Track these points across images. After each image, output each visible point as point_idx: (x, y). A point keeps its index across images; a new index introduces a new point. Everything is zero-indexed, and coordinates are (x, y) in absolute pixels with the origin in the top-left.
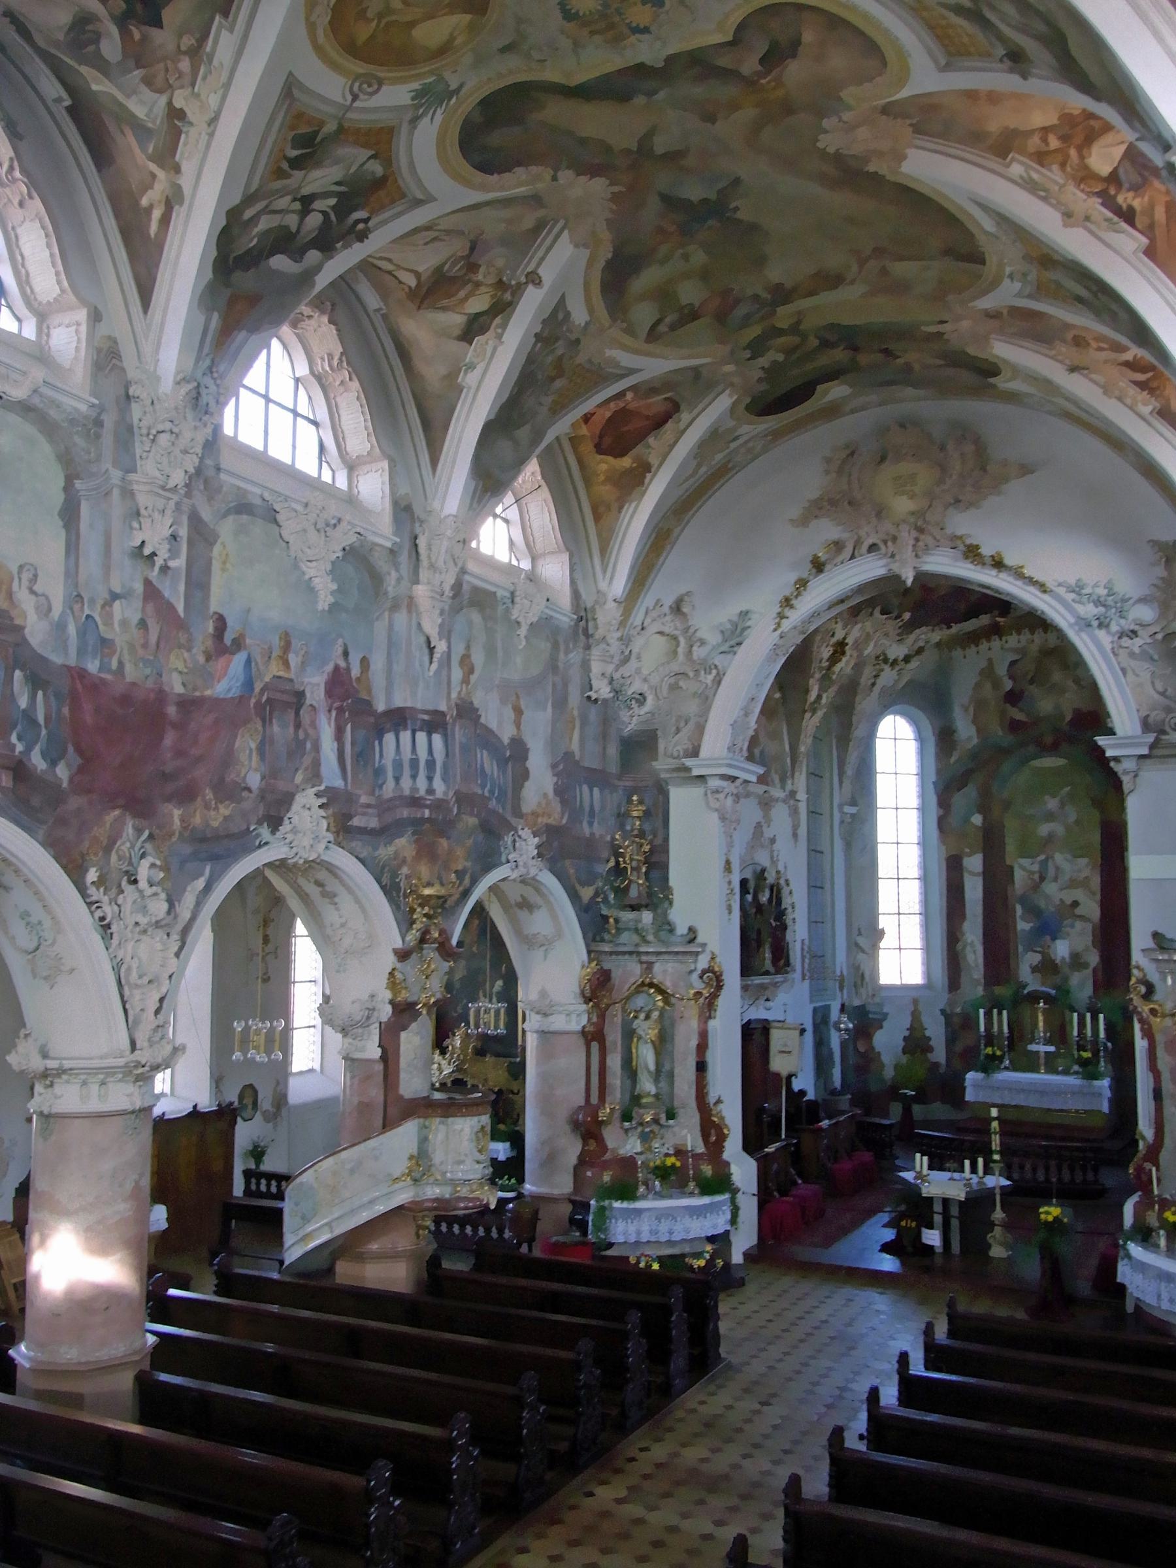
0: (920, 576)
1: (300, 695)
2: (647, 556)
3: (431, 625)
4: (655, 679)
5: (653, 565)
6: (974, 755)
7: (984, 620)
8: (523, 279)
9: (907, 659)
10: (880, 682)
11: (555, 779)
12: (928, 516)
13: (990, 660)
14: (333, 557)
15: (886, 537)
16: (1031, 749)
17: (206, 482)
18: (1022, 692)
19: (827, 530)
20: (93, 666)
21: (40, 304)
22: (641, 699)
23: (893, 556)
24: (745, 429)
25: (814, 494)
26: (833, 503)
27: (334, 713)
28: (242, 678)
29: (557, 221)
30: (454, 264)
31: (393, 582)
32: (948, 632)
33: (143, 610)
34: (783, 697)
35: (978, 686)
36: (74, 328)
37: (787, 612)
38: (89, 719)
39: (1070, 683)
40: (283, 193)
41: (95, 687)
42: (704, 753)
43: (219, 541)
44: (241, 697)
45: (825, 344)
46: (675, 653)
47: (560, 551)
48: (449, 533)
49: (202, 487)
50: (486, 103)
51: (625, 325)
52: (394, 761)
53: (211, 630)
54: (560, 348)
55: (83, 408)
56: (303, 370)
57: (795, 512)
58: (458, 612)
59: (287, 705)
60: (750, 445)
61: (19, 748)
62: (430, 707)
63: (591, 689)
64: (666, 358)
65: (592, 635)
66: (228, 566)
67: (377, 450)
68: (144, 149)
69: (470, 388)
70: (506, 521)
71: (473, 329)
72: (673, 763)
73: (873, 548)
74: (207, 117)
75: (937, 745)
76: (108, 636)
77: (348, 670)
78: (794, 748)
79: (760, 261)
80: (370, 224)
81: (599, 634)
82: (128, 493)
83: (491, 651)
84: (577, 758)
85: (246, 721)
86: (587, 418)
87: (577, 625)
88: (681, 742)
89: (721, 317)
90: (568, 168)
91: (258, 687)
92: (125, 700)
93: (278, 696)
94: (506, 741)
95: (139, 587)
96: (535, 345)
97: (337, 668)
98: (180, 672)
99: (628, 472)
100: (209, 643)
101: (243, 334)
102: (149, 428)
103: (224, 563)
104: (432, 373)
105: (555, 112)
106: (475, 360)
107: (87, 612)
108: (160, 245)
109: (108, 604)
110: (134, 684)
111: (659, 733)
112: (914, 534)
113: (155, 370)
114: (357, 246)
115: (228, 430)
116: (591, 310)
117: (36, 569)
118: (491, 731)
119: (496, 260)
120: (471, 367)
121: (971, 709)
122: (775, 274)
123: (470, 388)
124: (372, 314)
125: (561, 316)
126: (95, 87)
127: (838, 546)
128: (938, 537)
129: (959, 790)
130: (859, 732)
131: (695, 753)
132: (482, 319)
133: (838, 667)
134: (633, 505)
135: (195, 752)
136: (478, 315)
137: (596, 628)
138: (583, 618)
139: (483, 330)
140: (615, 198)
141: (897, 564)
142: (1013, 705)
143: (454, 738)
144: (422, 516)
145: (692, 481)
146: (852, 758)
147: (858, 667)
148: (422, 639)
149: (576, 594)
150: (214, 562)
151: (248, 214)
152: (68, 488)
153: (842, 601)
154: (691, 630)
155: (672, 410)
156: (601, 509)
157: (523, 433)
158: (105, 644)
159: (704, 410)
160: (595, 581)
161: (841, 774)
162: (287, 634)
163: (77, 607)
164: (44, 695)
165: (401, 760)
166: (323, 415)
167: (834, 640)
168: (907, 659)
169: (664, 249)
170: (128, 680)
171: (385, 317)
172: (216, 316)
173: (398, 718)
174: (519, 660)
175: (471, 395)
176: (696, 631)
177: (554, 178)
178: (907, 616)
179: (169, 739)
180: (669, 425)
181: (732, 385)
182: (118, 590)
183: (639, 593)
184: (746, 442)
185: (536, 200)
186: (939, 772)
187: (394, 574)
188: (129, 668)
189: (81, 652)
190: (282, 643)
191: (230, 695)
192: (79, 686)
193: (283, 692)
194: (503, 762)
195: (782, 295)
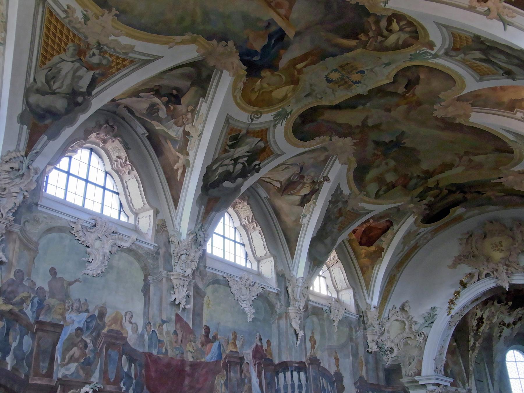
0: (511, 286)
1: (242, 358)
2: (386, 287)
3: (296, 324)
4: (397, 341)
5: (390, 291)
8: (322, 180)
10: (503, 335)
11: (356, 390)
12: (510, 259)
14: (253, 298)
15: (493, 270)
17: (200, 272)
19: (465, 269)
20: (155, 352)
21: (136, 210)
22: (391, 350)
23: (497, 278)
24: (422, 230)
25: (457, 254)
26: (466, 257)
27: (257, 365)
28: (217, 353)
30: (294, 177)
31: (279, 307)
33: (175, 327)
34: (458, 344)
36: (149, 217)
37: (453, 306)
38: (153, 374)
40: (226, 158)
41: (156, 361)
42: (423, 374)
43: (206, 296)
44: (217, 361)
45: (451, 192)
46: (404, 328)
47: (348, 288)
48: (300, 285)
49: (199, 275)
51: (365, 193)
52: (284, 386)
53: (203, 333)
54: (340, 205)
55: (152, 248)
56: (238, 224)
57: (450, 262)
58: (307, 318)
59: (236, 363)
60: (425, 236)
61: (124, 388)
62: (298, 360)
63: (368, 348)
64: (384, 204)
65: (367, 323)
66: (210, 305)
67: (268, 253)
68: (174, 148)
69: (305, 224)
70: (325, 278)
71: (304, 201)
72: (410, 379)
73: (487, 275)
74: (198, 134)
76: (161, 339)
77: (262, 346)
78: (467, 369)
79: (418, 162)
80: (261, 165)
81: (369, 322)
82: (169, 280)
83: (322, 334)
84: (366, 379)
85: (219, 372)
86: (354, 232)
87: (359, 319)
88: (412, 369)
89: (405, 186)
91: (224, 356)
92: (168, 365)
93: (232, 359)
94: (333, 374)
95: (174, 317)
96: (330, 204)
97: (257, 346)
98: (191, 352)
99: (375, 252)
100: (203, 339)
101: (214, 212)
102: (177, 253)
103: (209, 305)
104: (289, 220)
106: (306, 214)
107: (152, 329)
108: (181, 183)
109: (161, 325)
110: (172, 358)
111: (402, 365)
112: (505, 267)
113: (179, 231)
114: (256, 174)
115: (209, 251)
117: (132, 313)
118: (325, 369)
119: (311, 173)
120: (305, 216)
122: (425, 166)
123: (305, 224)
124: (264, 199)
125: (339, 192)
126: (157, 128)
127: (471, 275)
128: (517, 268)
130: (497, 359)
131: (419, 373)
132: (308, 196)
133: (481, 329)
134: (378, 265)
135: (198, 386)
136: (305, 196)
137: (368, 320)
138: (362, 316)
139: (308, 201)
140: (355, 144)
141: (500, 281)
143: (310, 373)
144: (289, 279)
145: (402, 253)
146: (496, 372)
147: (491, 328)
148: (293, 331)
149: (357, 306)
150: (204, 305)
151: (214, 167)
152: (145, 279)
153: (477, 300)
154: (410, 318)
155: (390, 224)
156: (365, 269)
157: (328, 241)
158: (160, 341)
159: (404, 223)
160: (365, 300)
161: (492, 380)
162: (235, 333)
163: (148, 327)
164: (135, 365)
165: (287, 385)
166: (246, 242)
167: (477, 317)
168: (514, 323)
169: (377, 162)
170: (169, 356)
171: (269, 200)
172: (203, 207)
173: (285, 366)
174: (335, 337)
175: (305, 227)
176: (412, 318)
177: (331, 140)
178: (510, 303)
179: (187, 382)
180: (389, 231)
181: (414, 212)
182: (165, 319)
183: (385, 303)
184: (423, 235)
185: (324, 149)
187: (279, 304)
188: (170, 352)
189: (150, 346)
190: (233, 337)
191: (212, 360)
192: (149, 361)
193: (235, 357)
194: (332, 383)
195: (429, 174)
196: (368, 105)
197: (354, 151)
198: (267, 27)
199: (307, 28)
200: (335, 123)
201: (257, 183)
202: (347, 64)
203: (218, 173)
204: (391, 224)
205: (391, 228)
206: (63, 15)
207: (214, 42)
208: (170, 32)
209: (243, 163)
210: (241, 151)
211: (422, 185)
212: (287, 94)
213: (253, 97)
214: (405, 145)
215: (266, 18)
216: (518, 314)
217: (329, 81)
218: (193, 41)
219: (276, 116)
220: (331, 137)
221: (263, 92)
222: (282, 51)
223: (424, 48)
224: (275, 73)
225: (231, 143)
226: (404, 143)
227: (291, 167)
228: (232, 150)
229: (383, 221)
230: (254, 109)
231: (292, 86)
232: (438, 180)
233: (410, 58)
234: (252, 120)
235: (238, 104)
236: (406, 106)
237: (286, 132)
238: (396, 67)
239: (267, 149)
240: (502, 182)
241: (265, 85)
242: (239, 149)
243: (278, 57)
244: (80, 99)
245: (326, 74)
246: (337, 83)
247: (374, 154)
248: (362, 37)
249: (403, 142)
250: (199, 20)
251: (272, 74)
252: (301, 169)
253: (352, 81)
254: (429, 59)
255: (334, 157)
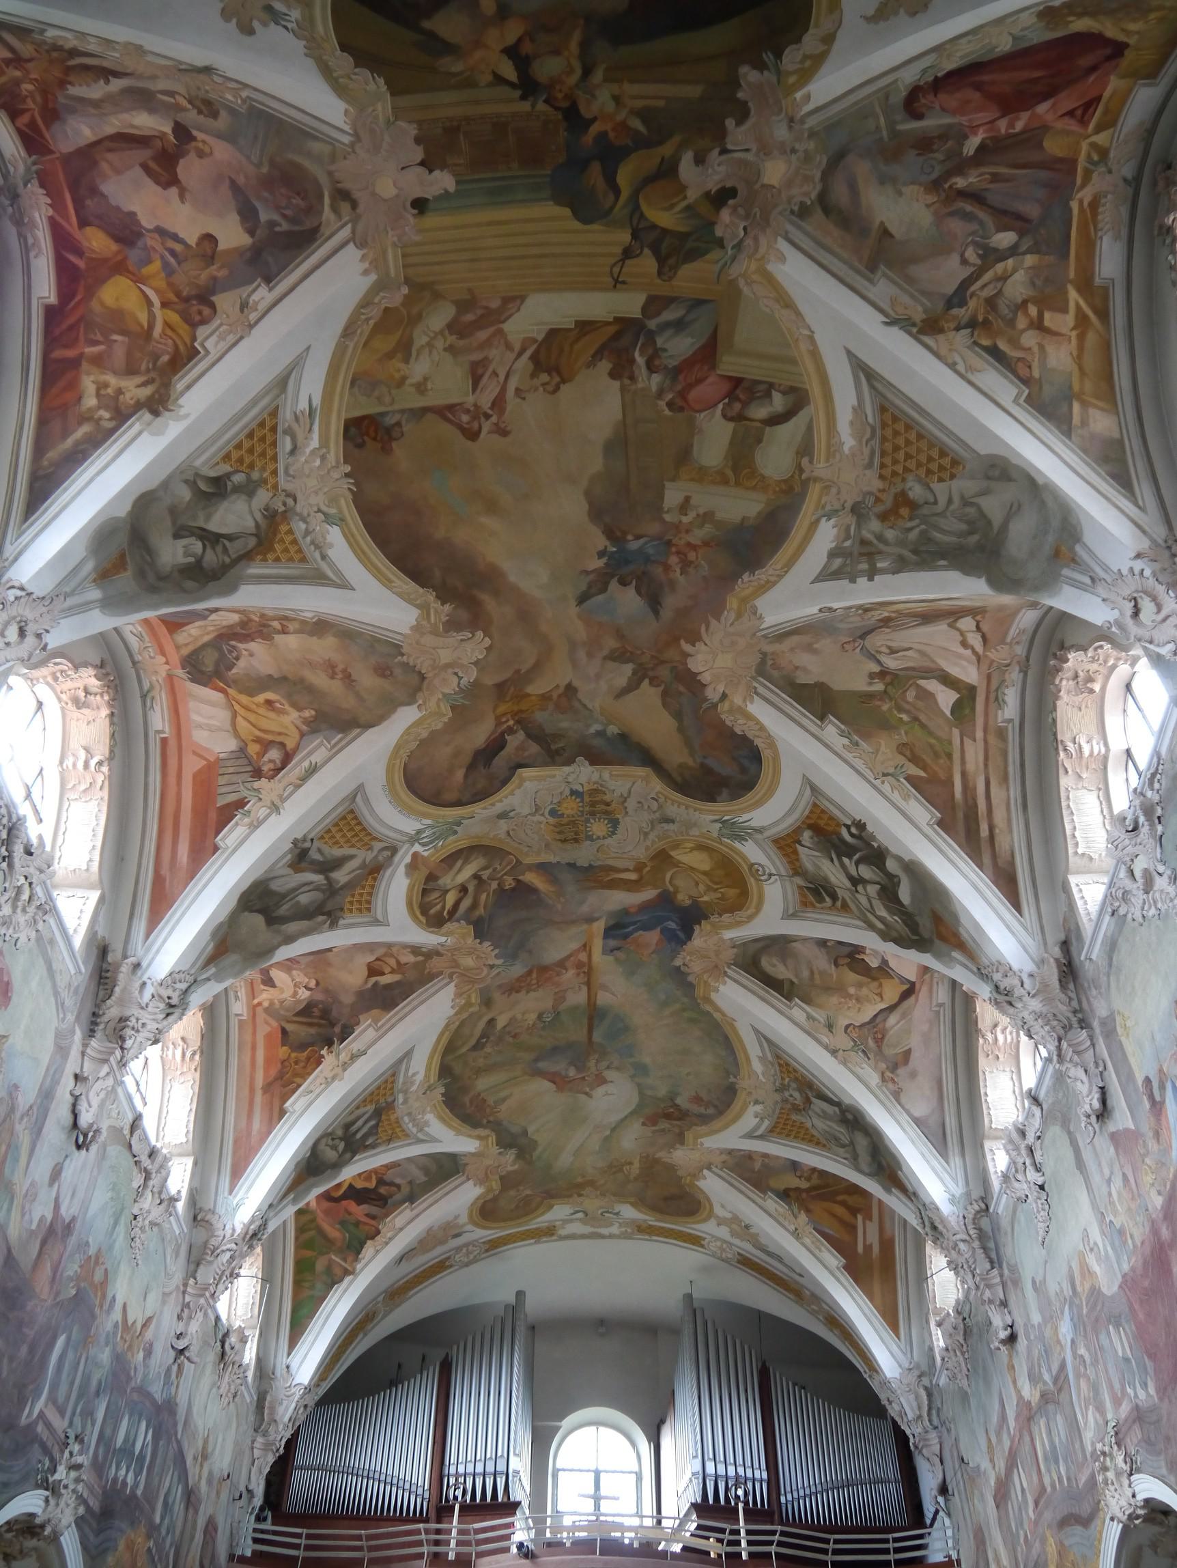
29: (765, 636)
50: (711, 798)
51: (805, 461)
64: (811, 339)
80: (849, 823)
90: (706, 700)
96: (883, 571)
105: (676, 755)
116: (814, 525)
125: (838, 562)
140: (694, 638)
157: (993, 507)
169: (697, 536)
177: (724, 696)
180: (949, 66)
181: (791, 120)
196: (595, 727)
197: (713, 622)
198: (618, 949)
199: (573, 922)
200: (681, 730)
201: (1008, 640)
202: (564, 841)
203: (889, 918)
204: (915, 93)
205: (931, 78)
206: (766, 1123)
207: (691, 978)
208: (717, 1026)
209: (857, 864)
210: (833, 872)
211: (669, 301)
212: (692, 849)
213: (732, 893)
214: (601, 542)
215: (610, 958)
217: (615, 823)
218: (708, 1000)
219: (741, 839)
220: (715, 706)
221: (717, 883)
222: (632, 910)
223: (426, 854)
224: (671, 889)
225: (828, 899)
226: (601, 554)
227: (884, 649)
228: (840, 893)
229: (932, 122)
230: (752, 882)
231: (673, 853)
232: (617, 283)
233: (459, 824)
234: (771, 875)
235: (758, 909)
236: (530, 689)
237: (759, 803)
238: (493, 805)
239: (812, 822)
240: (422, 164)
241: (702, 888)
242: (833, 879)
243: (645, 907)
244: (850, 1117)
245: (609, 841)
246: (607, 813)
247: (686, 565)
248: (509, 883)
249: (600, 563)
250: (677, 1006)
251: (676, 892)
252: (863, 636)
253: (582, 801)
254: (430, 826)
255: (763, 633)
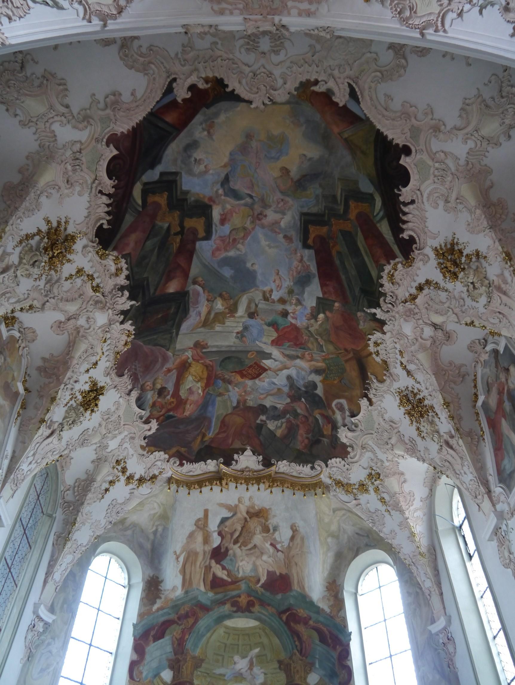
6: (176, 606)
7: (211, 465)
9: (141, 480)
13: (206, 512)
16: (227, 608)
18: (227, 550)
32: (180, 469)
35: (191, 536)
39: (268, 545)
75: (144, 590)
121: (181, 559)
129: (154, 641)
142: (218, 562)
147: (98, 462)
161: (48, 574)
168: (141, 480)
186: (141, 615)
216: (153, 465)
